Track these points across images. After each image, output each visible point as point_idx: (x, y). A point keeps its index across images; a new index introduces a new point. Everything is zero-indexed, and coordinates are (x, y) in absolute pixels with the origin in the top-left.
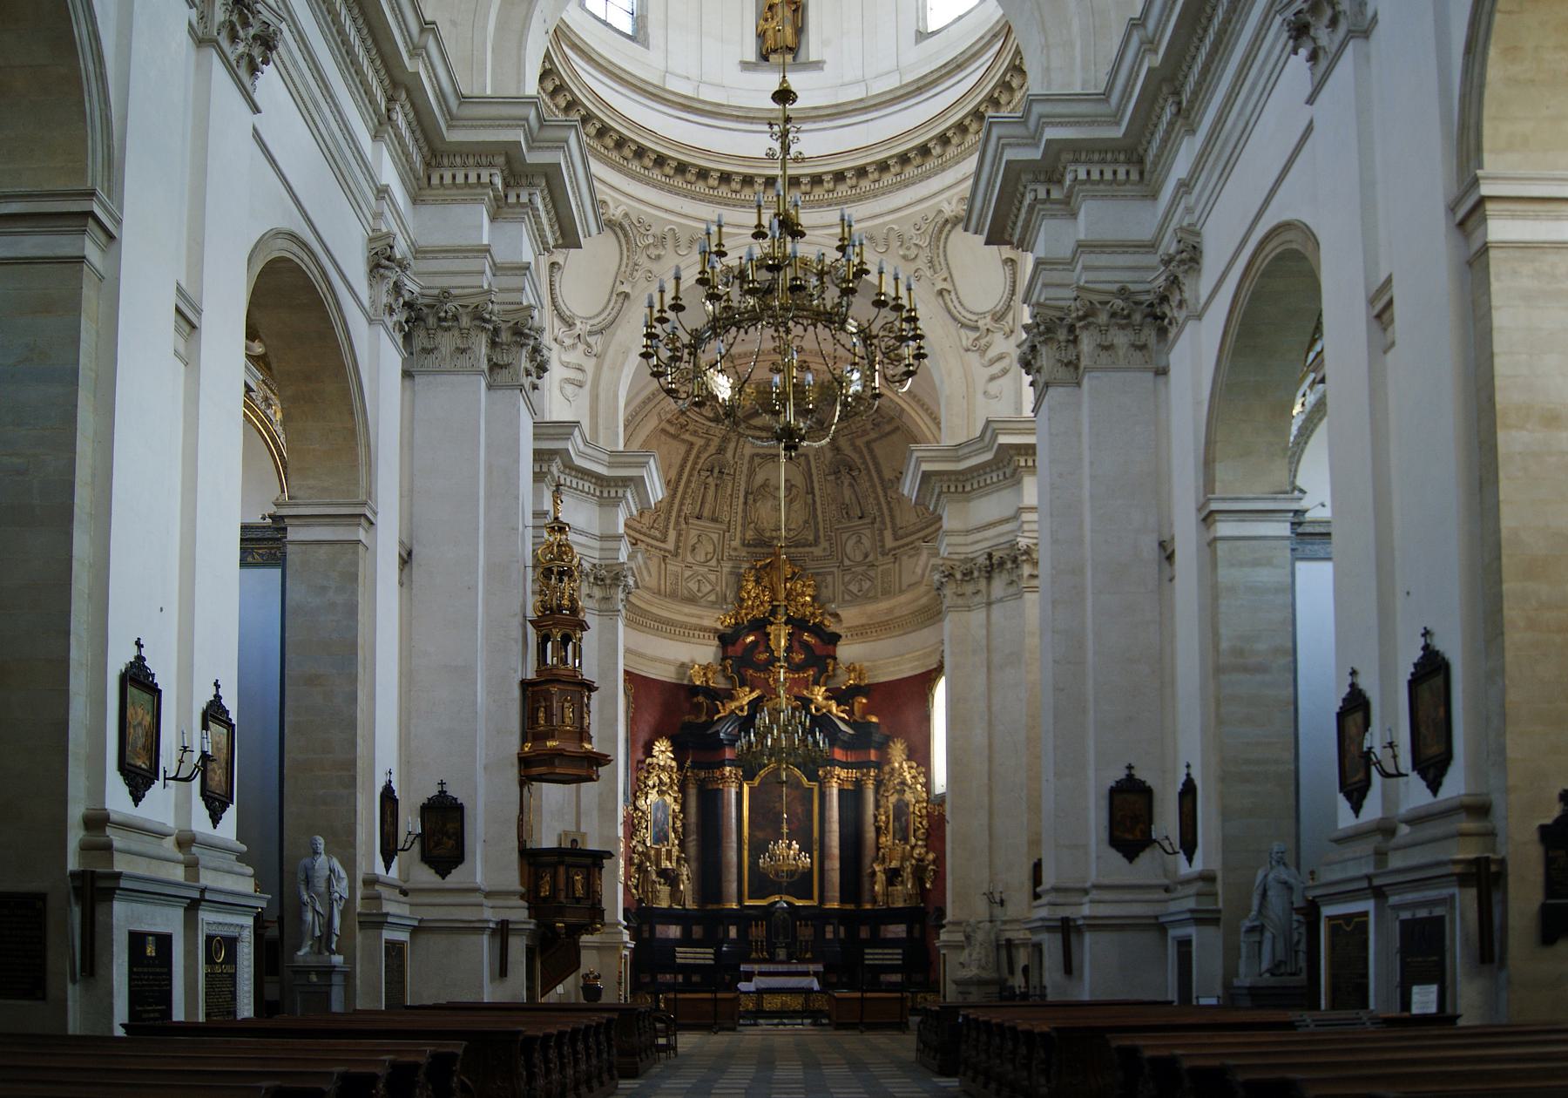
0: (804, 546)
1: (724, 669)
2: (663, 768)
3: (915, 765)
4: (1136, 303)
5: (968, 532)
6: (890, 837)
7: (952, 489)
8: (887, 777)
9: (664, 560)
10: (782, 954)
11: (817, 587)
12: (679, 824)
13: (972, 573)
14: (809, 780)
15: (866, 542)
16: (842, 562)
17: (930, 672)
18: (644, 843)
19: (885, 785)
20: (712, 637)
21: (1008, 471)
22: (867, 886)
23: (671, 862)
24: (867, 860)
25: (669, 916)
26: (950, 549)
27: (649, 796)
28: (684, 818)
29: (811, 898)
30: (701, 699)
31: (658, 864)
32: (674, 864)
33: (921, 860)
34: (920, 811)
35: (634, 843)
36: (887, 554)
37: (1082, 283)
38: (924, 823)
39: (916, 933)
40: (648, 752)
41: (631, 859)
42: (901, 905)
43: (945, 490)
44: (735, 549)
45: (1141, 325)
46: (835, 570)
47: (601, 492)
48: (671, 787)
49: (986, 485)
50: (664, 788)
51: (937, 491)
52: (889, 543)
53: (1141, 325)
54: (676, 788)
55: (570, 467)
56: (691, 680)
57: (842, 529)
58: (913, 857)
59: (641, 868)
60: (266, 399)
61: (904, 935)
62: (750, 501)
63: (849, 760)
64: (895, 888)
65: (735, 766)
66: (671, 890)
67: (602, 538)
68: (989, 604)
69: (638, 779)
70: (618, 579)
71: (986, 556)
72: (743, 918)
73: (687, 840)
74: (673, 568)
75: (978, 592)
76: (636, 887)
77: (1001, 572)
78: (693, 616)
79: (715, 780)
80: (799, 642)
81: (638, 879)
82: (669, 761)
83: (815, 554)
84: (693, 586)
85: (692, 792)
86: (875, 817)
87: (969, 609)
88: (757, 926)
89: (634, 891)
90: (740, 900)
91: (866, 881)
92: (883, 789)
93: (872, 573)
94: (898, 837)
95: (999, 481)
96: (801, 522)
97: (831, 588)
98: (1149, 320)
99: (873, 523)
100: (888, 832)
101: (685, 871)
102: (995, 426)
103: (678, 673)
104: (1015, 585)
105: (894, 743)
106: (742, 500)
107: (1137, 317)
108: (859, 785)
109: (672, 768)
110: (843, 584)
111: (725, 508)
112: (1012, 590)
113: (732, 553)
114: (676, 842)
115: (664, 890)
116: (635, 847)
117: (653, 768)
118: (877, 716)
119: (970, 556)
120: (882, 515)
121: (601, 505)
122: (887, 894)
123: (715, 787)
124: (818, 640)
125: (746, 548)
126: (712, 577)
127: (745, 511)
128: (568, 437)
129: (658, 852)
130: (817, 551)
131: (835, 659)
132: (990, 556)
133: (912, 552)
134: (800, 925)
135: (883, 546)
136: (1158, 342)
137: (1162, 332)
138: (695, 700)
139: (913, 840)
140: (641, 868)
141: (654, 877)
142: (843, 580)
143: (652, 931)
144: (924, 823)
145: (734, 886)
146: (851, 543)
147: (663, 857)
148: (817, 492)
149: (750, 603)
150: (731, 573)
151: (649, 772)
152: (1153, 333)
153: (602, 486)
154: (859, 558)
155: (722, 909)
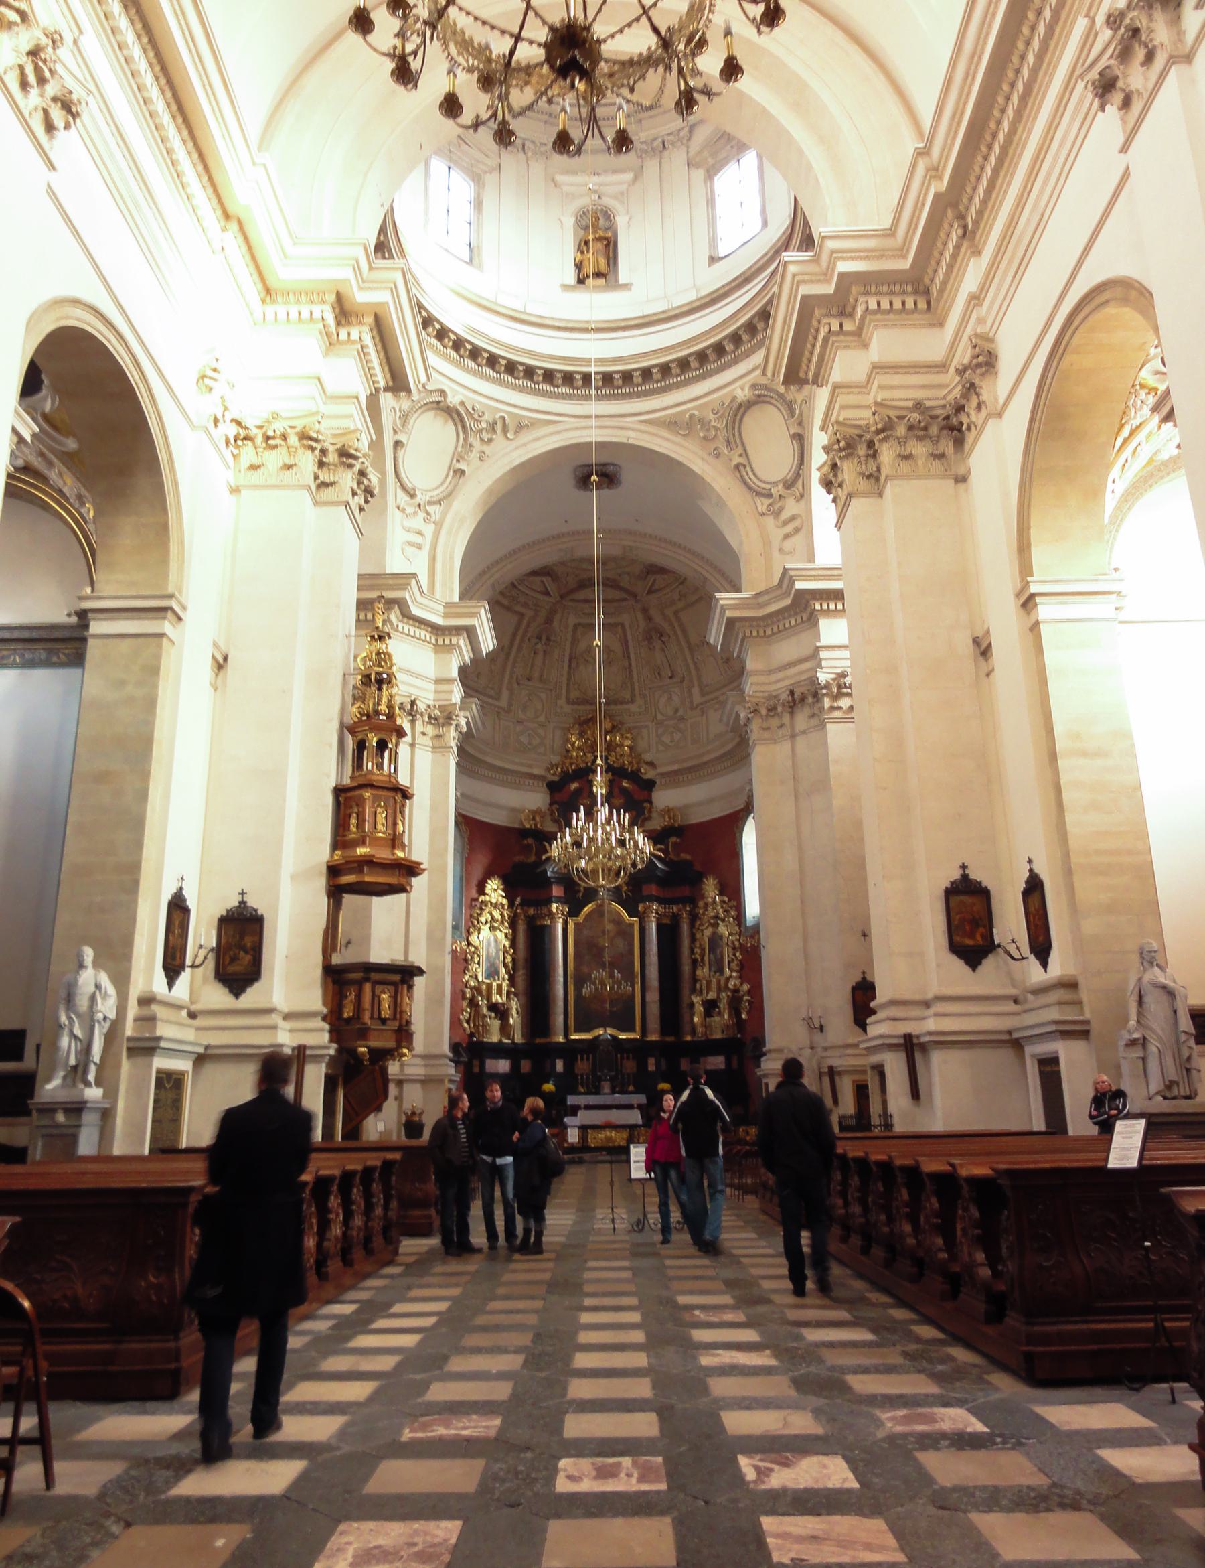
0: (621, 703)
1: (552, 813)
2: (495, 906)
3: (726, 899)
4: (932, 417)
5: (770, 672)
6: (706, 970)
7: (755, 633)
8: (701, 911)
10: (606, 1087)
11: (633, 739)
12: (509, 959)
13: (775, 708)
14: (630, 916)
15: (676, 699)
18: (476, 978)
19: (700, 919)
21: (805, 617)
22: (686, 1017)
23: (501, 996)
24: (686, 991)
25: (498, 1051)
26: (754, 688)
27: (482, 931)
28: (514, 953)
29: (632, 1030)
30: (530, 841)
31: (489, 998)
32: (504, 998)
33: (736, 991)
34: (733, 943)
35: (467, 977)
36: (696, 708)
37: (879, 400)
38: (738, 954)
39: (735, 1064)
40: (481, 890)
41: (464, 993)
42: (718, 1035)
43: (748, 633)
45: (938, 437)
46: (650, 724)
47: (437, 640)
48: (502, 923)
49: (785, 629)
50: (496, 925)
51: (741, 635)
52: (697, 699)
53: (938, 437)
54: (507, 924)
55: (407, 615)
56: (521, 822)
60: (80, 497)
61: (723, 1066)
62: (573, 665)
66: (502, 1025)
67: (438, 681)
68: (793, 737)
69: (471, 916)
70: (451, 719)
71: (788, 692)
72: (571, 1051)
73: (517, 975)
75: (781, 726)
76: (468, 1022)
77: (802, 706)
79: (542, 917)
81: (470, 1014)
82: (500, 899)
84: (524, 739)
85: (521, 928)
86: (692, 952)
87: (775, 742)
88: (582, 1059)
89: (466, 1025)
90: (566, 1035)
91: (685, 1011)
92: (698, 923)
94: (713, 969)
95: (797, 624)
98: (945, 432)
100: (704, 964)
101: (515, 1005)
102: (792, 573)
104: (816, 718)
107: (934, 430)
108: (676, 918)
109: (503, 905)
110: (657, 736)
112: (814, 722)
114: (507, 977)
115: (495, 1024)
116: (467, 981)
117: (486, 905)
119: (774, 694)
121: (436, 652)
122: (706, 1027)
126: (541, 732)
127: (569, 674)
128: (405, 587)
129: (489, 986)
130: (633, 708)
131: (651, 803)
132: (792, 693)
133: (717, 706)
134: (622, 1058)
135: (691, 702)
136: (955, 453)
137: (959, 443)
138: (525, 842)
139: (728, 972)
140: (473, 1003)
141: (485, 1011)
144: (738, 954)
145: (560, 1020)
146: (663, 700)
147: (494, 991)
148: (632, 656)
149: (574, 754)
151: (481, 909)
152: (951, 444)
153: (437, 635)
154: (670, 712)
155: (550, 1043)
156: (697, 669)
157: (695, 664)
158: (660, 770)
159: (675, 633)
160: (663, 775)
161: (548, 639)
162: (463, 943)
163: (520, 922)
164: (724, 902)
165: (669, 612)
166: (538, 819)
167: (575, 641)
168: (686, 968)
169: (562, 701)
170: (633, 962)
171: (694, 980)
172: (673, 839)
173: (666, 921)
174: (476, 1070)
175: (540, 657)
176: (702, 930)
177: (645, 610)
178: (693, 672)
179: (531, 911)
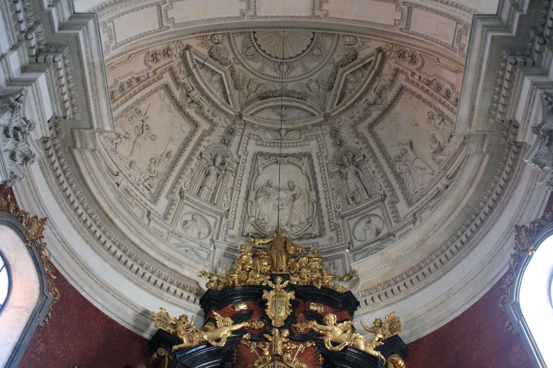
9: (147, 216)
16: (351, 243)
17: (501, 282)
20: (192, 298)
44: (232, 237)
78: (170, 258)
80: (304, 312)
96: (304, 219)
99: (383, 200)
103: (137, 321)
106: (243, 195)
113: (228, 239)
120: (392, 189)
125: (244, 238)
130: (323, 242)
135: (397, 216)
148: (321, 188)
150: (225, 255)
156: (401, 183)
157: (398, 176)
159: (372, 151)
161: (223, 164)
165: (362, 128)
167: (254, 174)
177: (335, 133)
178: (396, 186)
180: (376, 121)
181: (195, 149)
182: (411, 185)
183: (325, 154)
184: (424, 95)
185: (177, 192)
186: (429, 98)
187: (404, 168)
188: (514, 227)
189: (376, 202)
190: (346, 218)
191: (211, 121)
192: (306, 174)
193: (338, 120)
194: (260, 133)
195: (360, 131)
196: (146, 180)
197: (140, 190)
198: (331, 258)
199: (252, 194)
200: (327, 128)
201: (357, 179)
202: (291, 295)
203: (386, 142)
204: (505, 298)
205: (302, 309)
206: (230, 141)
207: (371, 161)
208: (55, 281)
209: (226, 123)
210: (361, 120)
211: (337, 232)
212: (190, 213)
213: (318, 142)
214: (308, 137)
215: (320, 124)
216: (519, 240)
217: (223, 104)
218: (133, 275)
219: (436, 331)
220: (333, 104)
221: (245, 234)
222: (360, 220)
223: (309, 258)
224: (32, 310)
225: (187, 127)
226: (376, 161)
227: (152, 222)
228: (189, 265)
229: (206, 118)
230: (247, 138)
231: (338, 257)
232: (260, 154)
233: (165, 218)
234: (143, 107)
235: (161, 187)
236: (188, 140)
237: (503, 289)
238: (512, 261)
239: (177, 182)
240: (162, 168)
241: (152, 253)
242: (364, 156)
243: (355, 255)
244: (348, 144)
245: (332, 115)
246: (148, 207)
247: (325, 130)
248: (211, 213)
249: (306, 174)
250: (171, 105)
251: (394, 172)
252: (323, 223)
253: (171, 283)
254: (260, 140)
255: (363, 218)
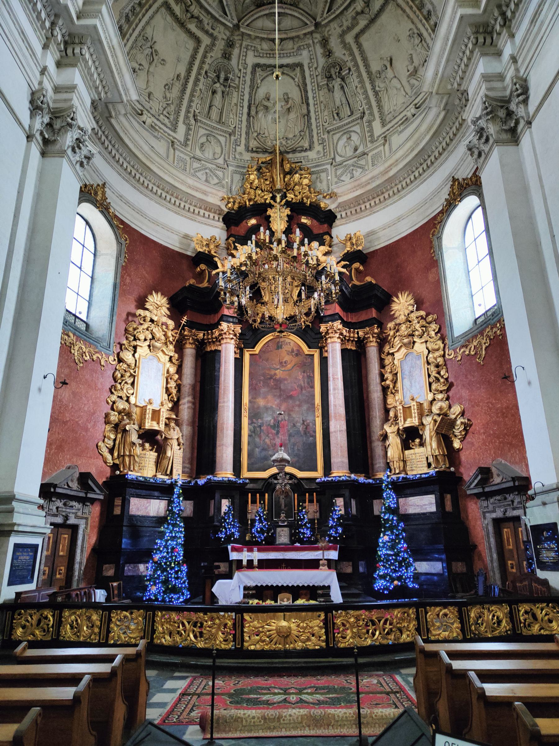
8: (392, 333)
9: (172, 146)
12: (172, 384)
14: (310, 348)
16: (334, 159)
17: (435, 218)
18: (128, 401)
20: (217, 218)
23: (158, 423)
27: (139, 349)
29: (315, 469)
30: (203, 267)
33: (444, 415)
35: (114, 398)
38: (442, 373)
39: (449, 507)
40: (141, 303)
41: (107, 415)
44: (241, 153)
46: (328, 167)
50: (158, 344)
52: (378, 129)
54: (171, 347)
57: (333, 130)
58: (431, 412)
59: (118, 427)
61: (433, 509)
62: (253, 113)
63: (350, 320)
64: (411, 451)
65: (234, 323)
66: (158, 457)
74: (182, 155)
76: (111, 451)
78: (197, 190)
81: (115, 440)
82: (165, 319)
83: (310, 157)
85: (190, 351)
89: (109, 457)
93: (362, 162)
96: (297, 132)
97: (325, 183)
99: (362, 118)
100: (397, 391)
101: (175, 434)
103: (181, 243)
105: (397, 297)
106: (246, 110)
108: (361, 343)
110: (336, 176)
111: (231, 116)
114: (170, 405)
116: (114, 403)
117: (144, 321)
118: (375, 279)
120: (370, 107)
123: (213, 348)
124: (315, 221)
126: (220, 174)
127: (248, 121)
129: (143, 409)
130: (312, 155)
135: (372, 136)
140: (118, 427)
141: (134, 437)
142: (336, 174)
143: (125, 505)
147: (149, 415)
148: (311, 101)
154: (349, 152)
156: (379, 101)
157: (376, 93)
158: (340, 200)
159: (356, 65)
160: (343, 206)
161: (226, 79)
162: (111, 358)
163: (188, 346)
164: (422, 317)
165: (350, 38)
166: (212, 246)
168: (376, 394)
169: (241, 148)
170: (313, 396)
171: (387, 411)
172: (356, 265)
173: (351, 346)
174: (117, 511)
175: (218, 96)
176: (393, 354)
177: (325, 42)
178: (374, 104)
179: (201, 335)
180: (363, 31)
181: (200, 68)
182: (386, 104)
183: (315, 65)
184: (408, 10)
185: (191, 115)
186: (412, 15)
187: (382, 85)
188: (451, 178)
189: (356, 120)
190: (331, 133)
191: (211, 35)
192: (299, 86)
193: (328, 29)
194: (256, 43)
195: (347, 42)
196: (165, 109)
197: (162, 120)
198: (318, 172)
199: (253, 109)
200: (317, 36)
201: (342, 93)
202: (287, 211)
203: (370, 55)
204: (434, 231)
205: (296, 221)
206: (230, 55)
207: (355, 75)
208: (123, 229)
209: (225, 35)
210: (349, 29)
211: (324, 146)
212: (204, 135)
213: (309, 51)
214: (300, 46)
215: (311, 33)
216: (453, 190)
217: (221, 16)
218: (173, 206)
219: (387, 246)
220: (323, 12)
221: (250, 149)
222: (342, 135)
223: (301, 175)
224: (115, 256)
225: (191, 44)
226: (360, 76)
227: (176, 151)
228: (212, 193)
229: (207, 32)
230: (245, 50)
231: (323, 171)
232: (257, 65)
233: (186, 145)
234: (149, 31)
235: (178, 113)
236: (193, 58)
237: (435, 224)
238: (445, 203)
239: (189, 106)
240: (175, 92)
241: (183, 188)
242: (350, 69)
243: (336, 170)
244: (336, 55)
245: (323, 23)
246: (171, 138)
247: (316, 38)
248: (221, 133)
249: (299, 86)
250: (174, 24)
251: (374, 88)
252: (313, 136)
253: (200, 208)
254: (257, 51)
255: (345, 133)
